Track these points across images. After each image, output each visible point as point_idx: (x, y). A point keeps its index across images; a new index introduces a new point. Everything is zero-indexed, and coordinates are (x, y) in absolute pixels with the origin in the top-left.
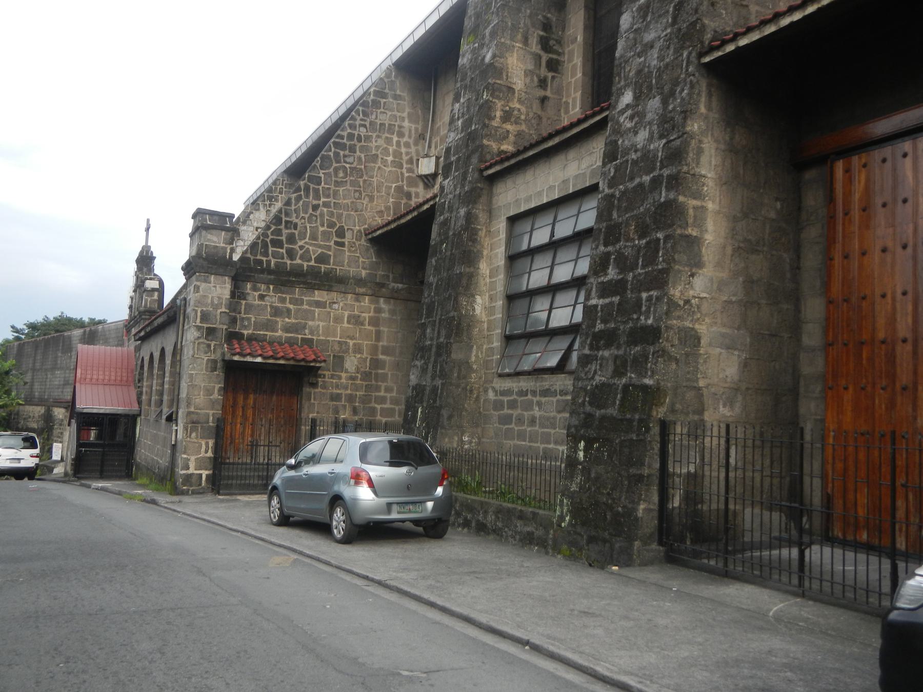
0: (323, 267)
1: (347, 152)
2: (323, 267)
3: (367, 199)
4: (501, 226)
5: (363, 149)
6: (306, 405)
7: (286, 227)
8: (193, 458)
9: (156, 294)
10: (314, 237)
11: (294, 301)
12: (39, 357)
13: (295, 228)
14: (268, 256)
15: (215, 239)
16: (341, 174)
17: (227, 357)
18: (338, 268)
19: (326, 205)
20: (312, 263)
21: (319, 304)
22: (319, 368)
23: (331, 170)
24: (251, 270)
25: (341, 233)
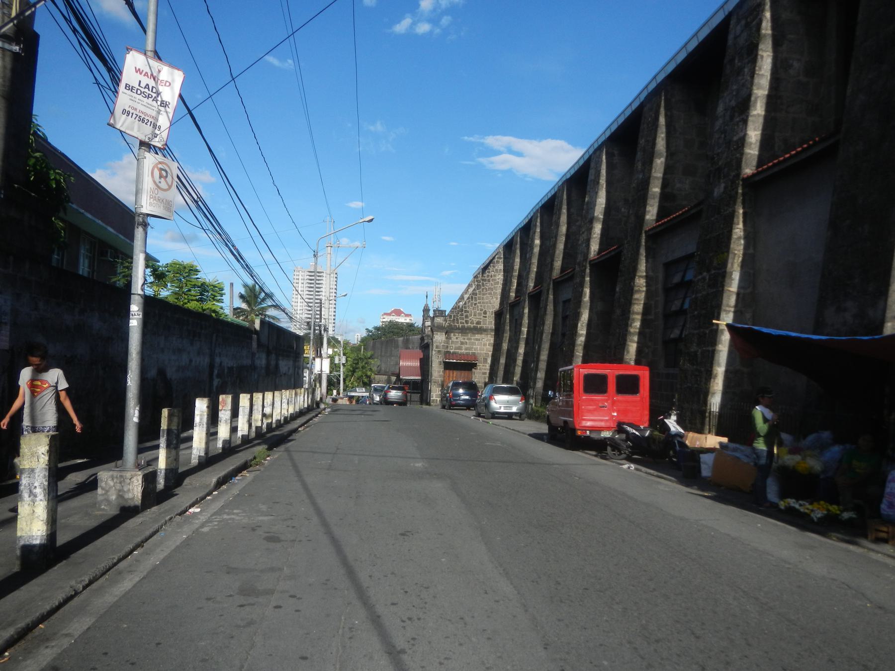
0: (479, 326)
1: (487, 282)
2: (479, 326)
3: (495, 299)
4: (514, 321)
5: (493, 280)
6: (473, 376)
7: (465, 313)
8: (434, 394)
9: (430, 328)
10: (475, 315)
11: (469, 339)
12: (383, 350)
13: (468, 313)
14: (458, 323)
15: (439, 320)
16: (485, 291)
17: (444, 360)
18: (484, 326)
19: (480, 303)
20: (475, 325)
21: (477, 340)
22: (477, 363)
23: (481, 290)
24: (452, 329)
25: (485, 313)
